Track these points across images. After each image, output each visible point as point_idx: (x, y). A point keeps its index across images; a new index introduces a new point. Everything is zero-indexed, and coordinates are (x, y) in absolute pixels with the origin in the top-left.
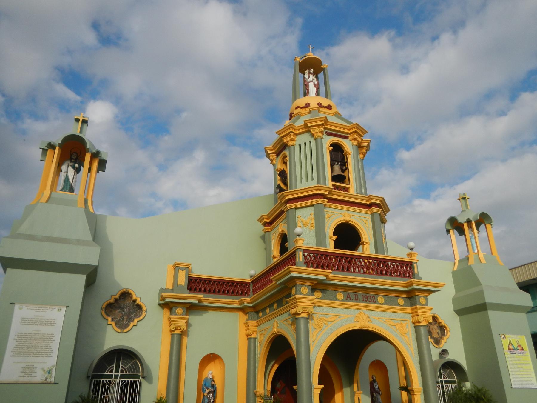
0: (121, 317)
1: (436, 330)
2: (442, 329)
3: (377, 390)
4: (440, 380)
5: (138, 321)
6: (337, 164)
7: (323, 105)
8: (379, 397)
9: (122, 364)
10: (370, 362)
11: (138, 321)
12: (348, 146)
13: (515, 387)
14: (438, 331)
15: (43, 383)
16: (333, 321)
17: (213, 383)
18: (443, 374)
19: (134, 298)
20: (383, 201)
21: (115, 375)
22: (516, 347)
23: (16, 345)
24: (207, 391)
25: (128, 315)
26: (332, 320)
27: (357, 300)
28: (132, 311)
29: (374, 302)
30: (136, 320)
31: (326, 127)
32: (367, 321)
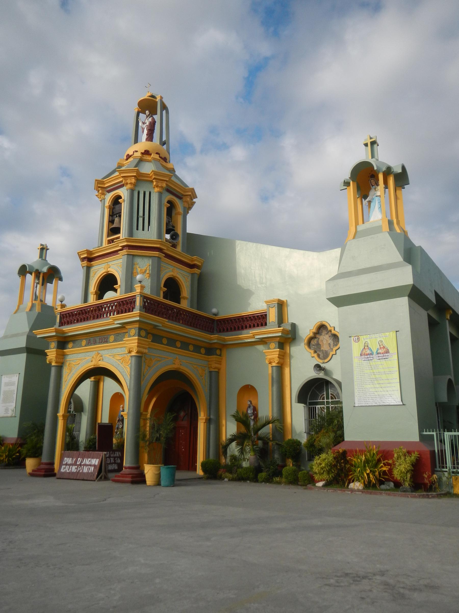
2: (335, 337)
4: (325, 400)
6: (117, 217)
7: (130, 155)
10: (239, 388)
12: (124, 193)
13: (359, 405)
14: (331, 341)
15: (11, 417)
16: (78, 364)
18: (331, 394)
20: (127, 240)
22: (375, 351)
23: (3, 398)
26: (78, 363)
27: (95, 343)
29: (107, 342)
31: (106, 186)
32: (98, 360)
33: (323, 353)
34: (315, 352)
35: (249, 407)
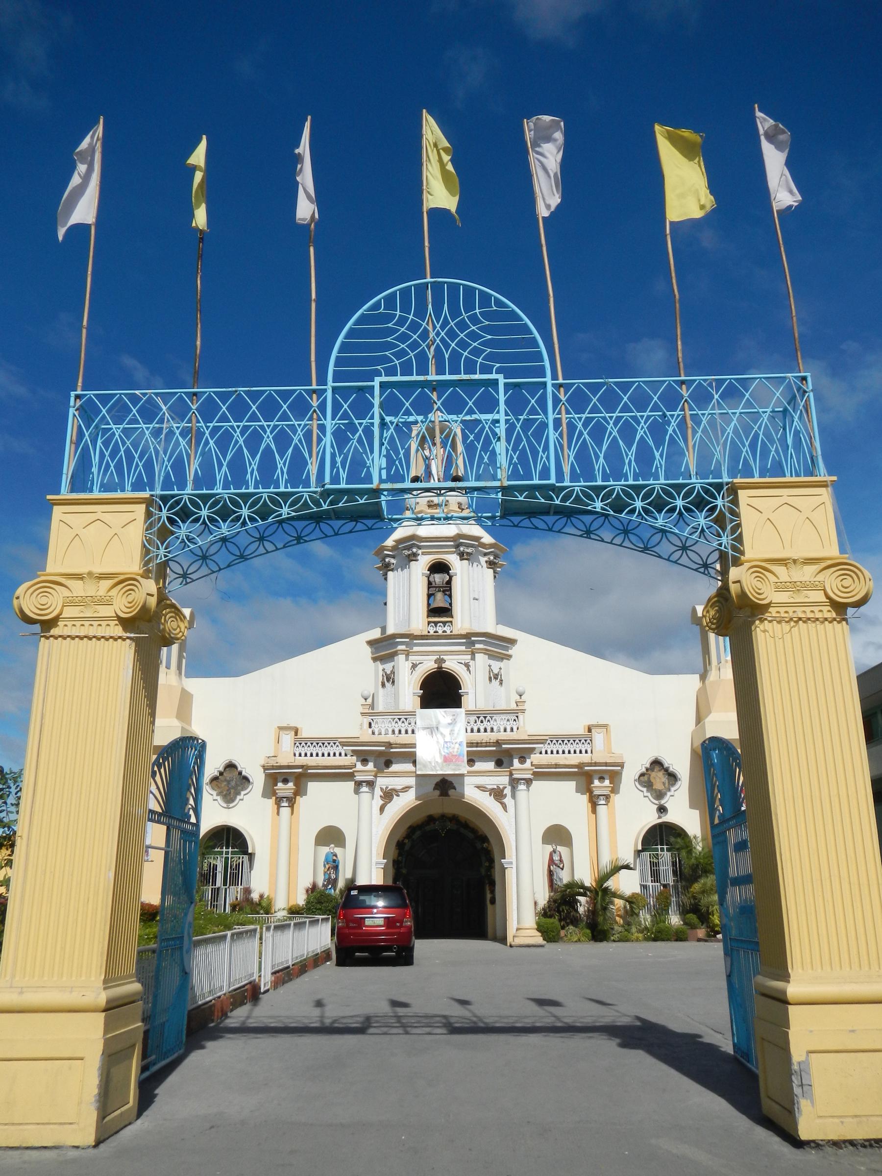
0: (228, 790)
1: (660, 778)
2: (672, 777)
3: (557, 862)
5: (245, 795)
6: (438, 591)
8: (559, 870)
9: (232, 840)
11: (245, 795)
14: (665, 779)
17: (335, 858)
19: (239, 769)
21: (226, 852)
24: (327, 866)
25: (235, 788)
28: (238, 783)
30: (243, 793)
33: (656, 792)
34: (648, 791)
35: (554, 851)
